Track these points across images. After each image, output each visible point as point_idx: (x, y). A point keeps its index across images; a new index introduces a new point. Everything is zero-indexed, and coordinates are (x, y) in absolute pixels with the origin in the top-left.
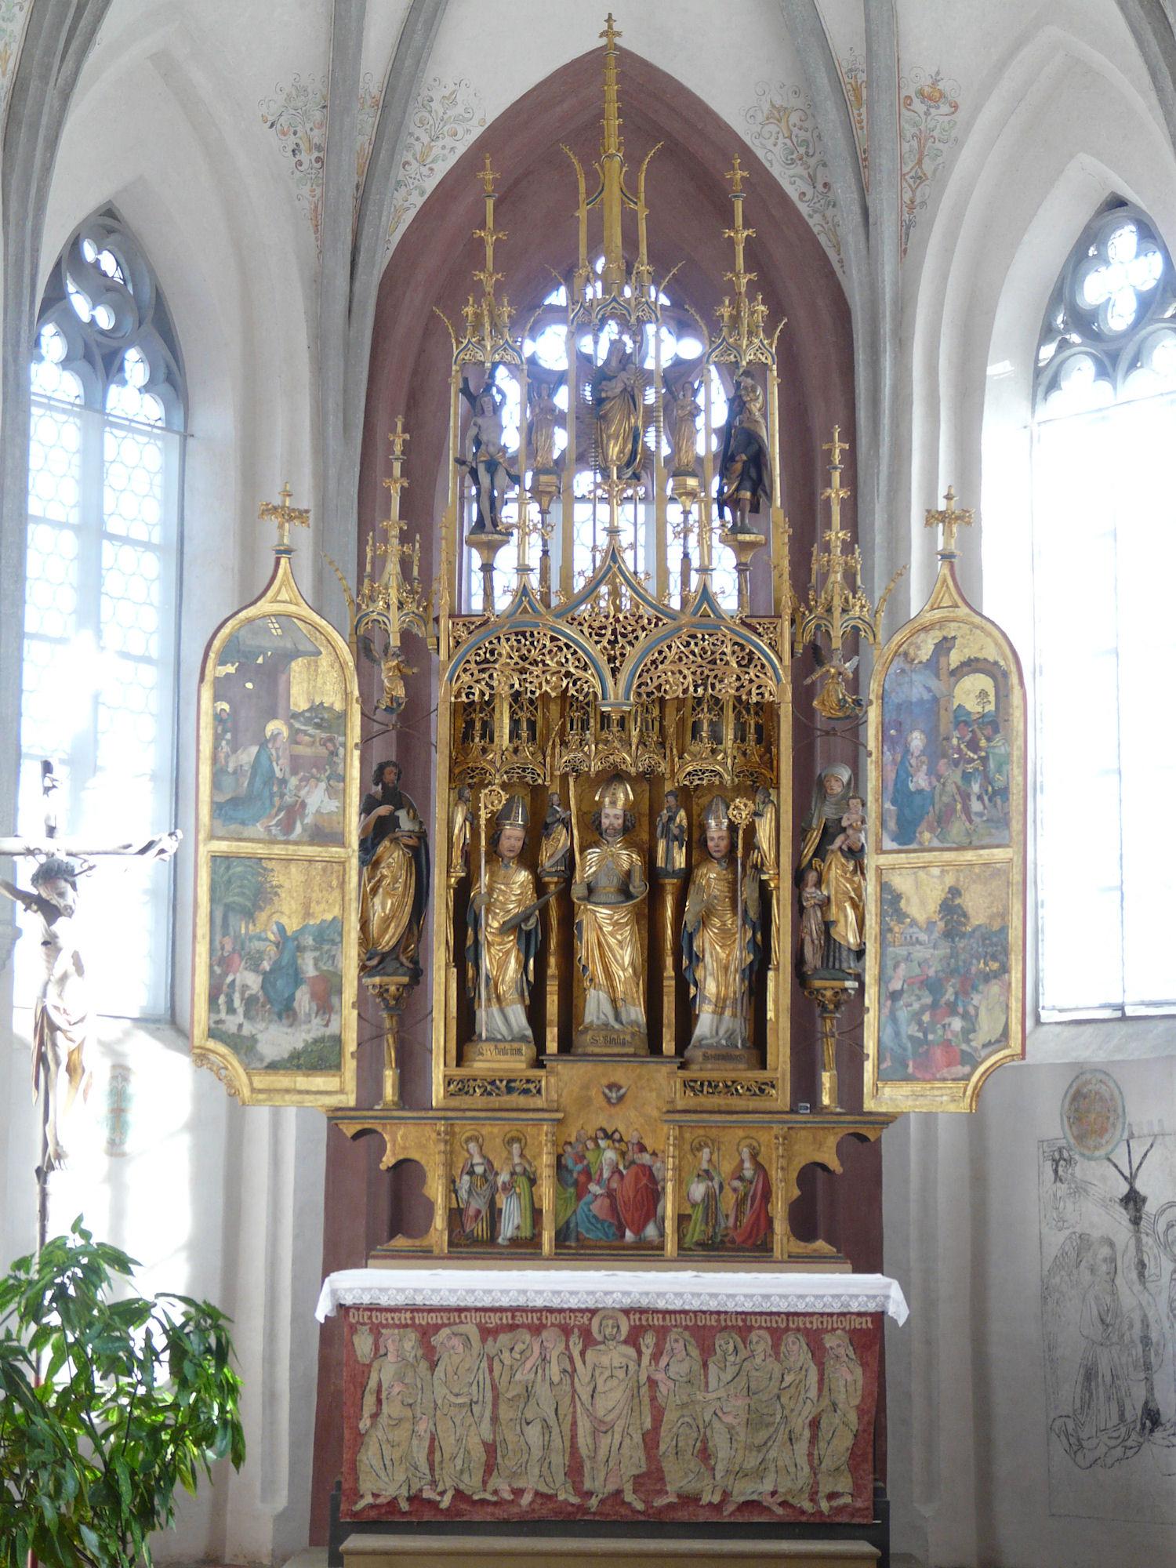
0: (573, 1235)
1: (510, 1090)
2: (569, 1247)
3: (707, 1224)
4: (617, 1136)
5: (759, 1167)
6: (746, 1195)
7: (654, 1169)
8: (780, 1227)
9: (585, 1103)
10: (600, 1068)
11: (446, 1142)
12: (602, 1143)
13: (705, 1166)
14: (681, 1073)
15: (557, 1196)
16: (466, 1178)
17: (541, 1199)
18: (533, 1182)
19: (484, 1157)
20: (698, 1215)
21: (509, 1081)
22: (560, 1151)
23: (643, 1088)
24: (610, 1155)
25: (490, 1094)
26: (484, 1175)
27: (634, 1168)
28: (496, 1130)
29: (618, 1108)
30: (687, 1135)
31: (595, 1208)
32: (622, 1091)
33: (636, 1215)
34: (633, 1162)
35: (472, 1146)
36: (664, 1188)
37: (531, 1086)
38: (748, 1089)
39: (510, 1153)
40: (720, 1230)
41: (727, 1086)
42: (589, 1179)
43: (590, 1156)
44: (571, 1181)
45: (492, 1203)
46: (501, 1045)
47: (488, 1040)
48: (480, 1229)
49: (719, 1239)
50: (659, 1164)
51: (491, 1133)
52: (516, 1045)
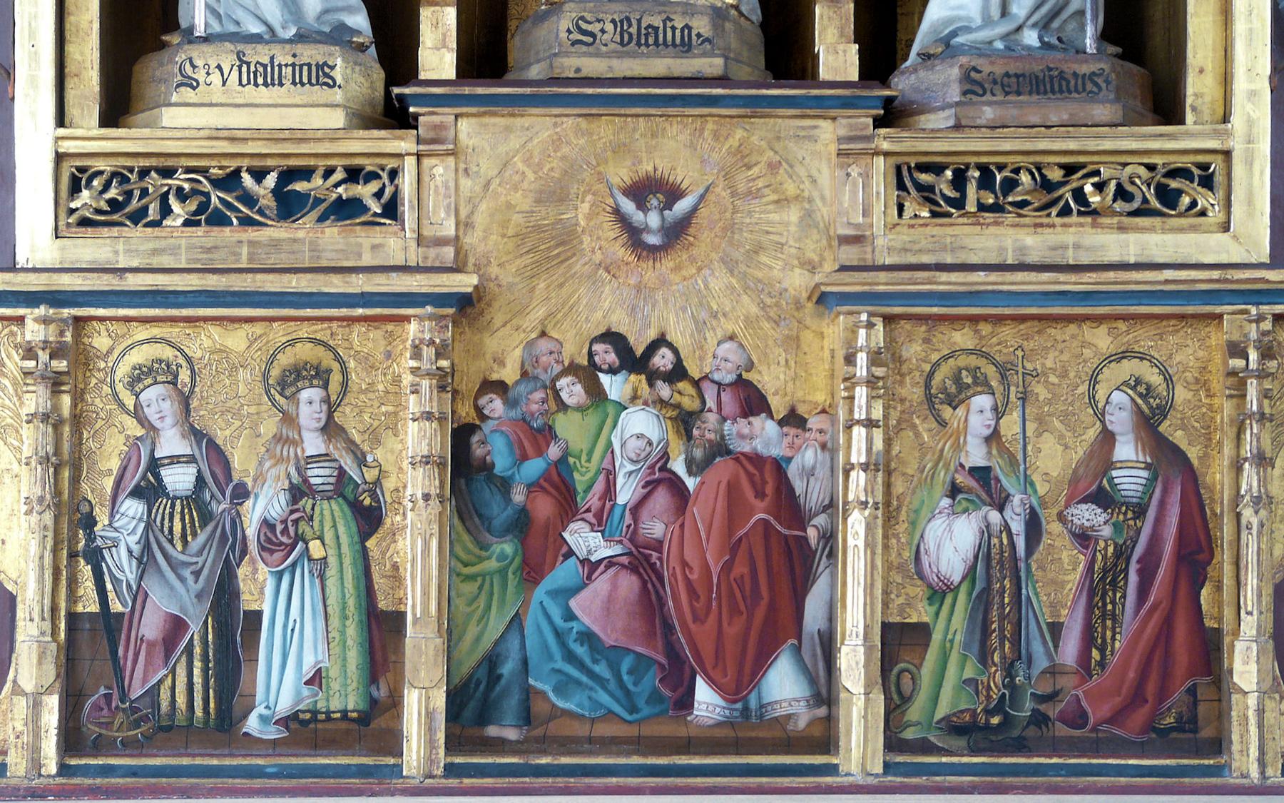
0: (512, 703)
1: (289, 206)
2: (499, 746)
3: (984, 658)
4: (663, 360)
5: (1166, 458)
6: (1122, 553)
7: (792, 471)
8: (1247, 666)
9: (551, 246)
10: (606, 129)
11: (56, 383)
12: (614, 386)
13: (976, 455)
14: (886, 140)
15: (457, 570)
16: (133, 508)
17: (395, 575)
18: (369, 518)
19: (197, 435)
20: (952, 625)
21: (289, 175)
22: (466, 412)
23: (754, 194)
24: (641, 425)
25: (218, 220)
26: (195, 499)
27: (723, 469)
28: (237, 340)
29: (667, 263)
30: (913, 350)
31: (588, 607)
32: (682, 206)
33: (732, 630)
34: (720, 449)
35: (155, 398)
36: (829, 537)
37: (365, 191)
38: (1122, 194)
39: (289, 419)
40: (1032, 681)
41: (1047, 185)
42: (568, 507)
43: (571, 429)
44: (500, 514)
45: (224, 595)
46: (258, 54)
47: (206, 39)
48: (182, 686)
49: (1029, 705)
50: (809, 456)
51: (223, 351)
52: (311, 54)
